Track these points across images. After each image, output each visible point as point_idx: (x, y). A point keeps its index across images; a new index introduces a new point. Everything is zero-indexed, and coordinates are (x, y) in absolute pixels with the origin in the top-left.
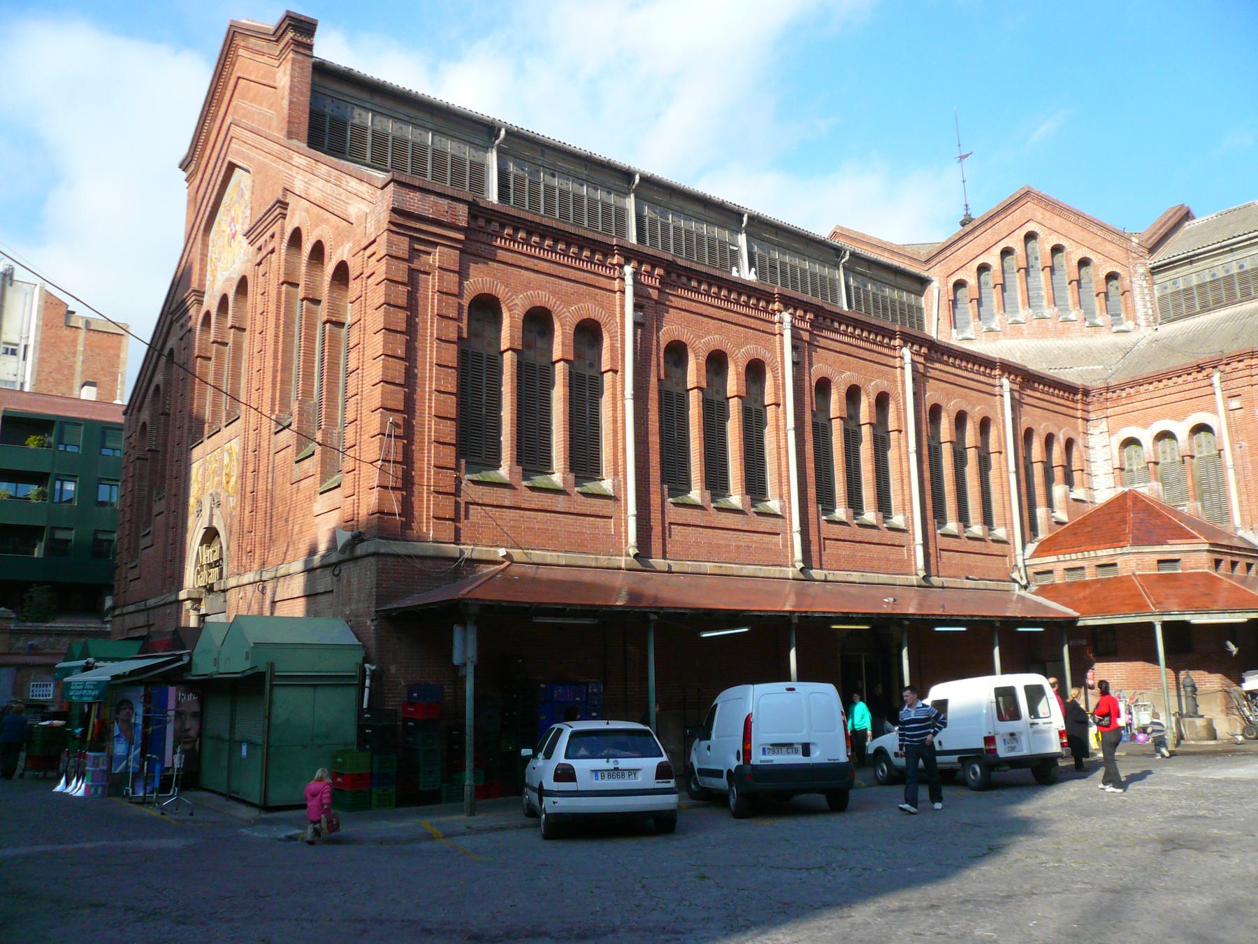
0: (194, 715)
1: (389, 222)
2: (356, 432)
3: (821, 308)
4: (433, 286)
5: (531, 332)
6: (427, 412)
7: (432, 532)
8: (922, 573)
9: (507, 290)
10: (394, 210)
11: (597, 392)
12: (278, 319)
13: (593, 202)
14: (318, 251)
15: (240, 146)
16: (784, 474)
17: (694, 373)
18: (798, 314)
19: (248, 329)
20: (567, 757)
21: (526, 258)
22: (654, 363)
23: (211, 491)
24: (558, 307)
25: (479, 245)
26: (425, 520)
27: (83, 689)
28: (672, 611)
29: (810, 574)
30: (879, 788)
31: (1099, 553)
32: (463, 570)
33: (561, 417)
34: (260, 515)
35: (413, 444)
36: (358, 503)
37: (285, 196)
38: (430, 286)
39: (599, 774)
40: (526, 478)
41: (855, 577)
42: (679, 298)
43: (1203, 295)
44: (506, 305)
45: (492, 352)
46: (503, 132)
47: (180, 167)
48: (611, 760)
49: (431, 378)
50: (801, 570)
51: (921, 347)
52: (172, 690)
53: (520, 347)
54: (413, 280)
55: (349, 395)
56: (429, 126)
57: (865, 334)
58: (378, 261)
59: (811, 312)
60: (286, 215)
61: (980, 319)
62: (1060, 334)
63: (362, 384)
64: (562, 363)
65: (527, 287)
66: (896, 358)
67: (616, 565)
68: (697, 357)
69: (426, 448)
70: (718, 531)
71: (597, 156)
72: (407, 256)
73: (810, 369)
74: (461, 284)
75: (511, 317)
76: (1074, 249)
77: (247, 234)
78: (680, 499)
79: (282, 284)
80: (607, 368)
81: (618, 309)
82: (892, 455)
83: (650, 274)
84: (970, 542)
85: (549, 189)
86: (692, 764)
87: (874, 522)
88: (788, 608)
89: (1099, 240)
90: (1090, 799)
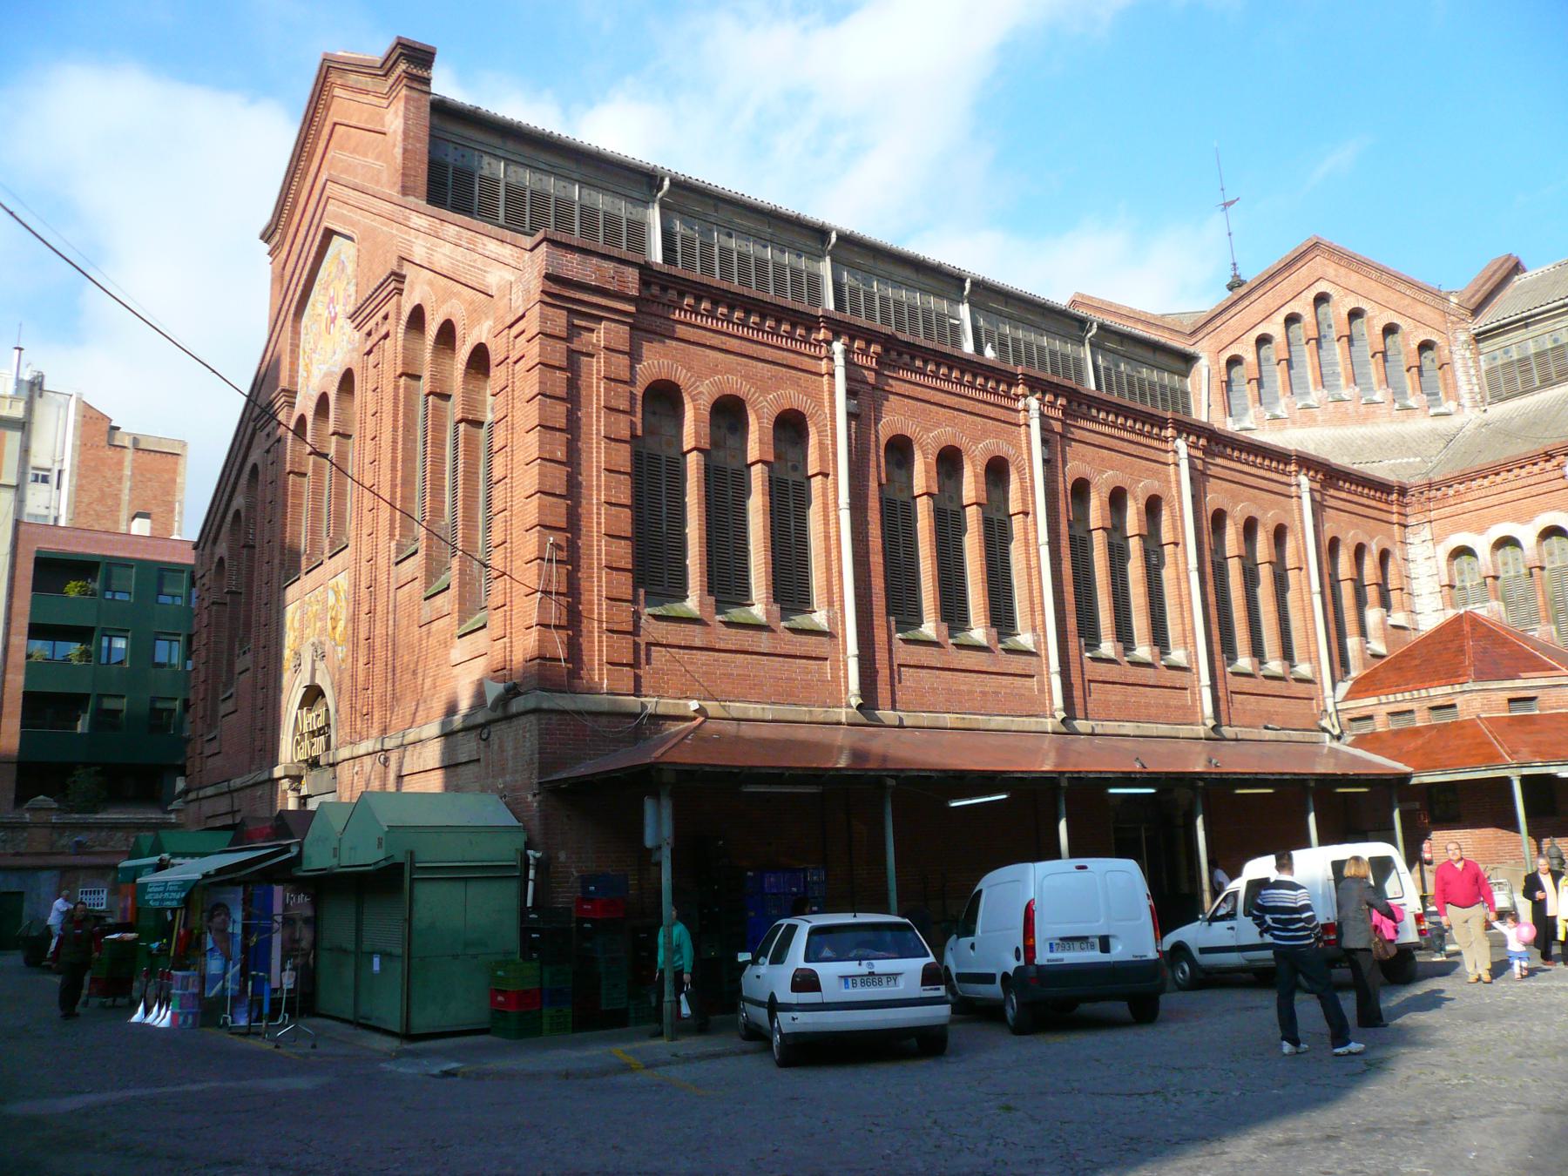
0: (307, 921)
1: (542, 291)
2: (506, 558)
3: (1075, 391)
4: (599, 372)
6: (595, 529)
7: (605, 681)
8: (1211, 723)
10: (548, 277)
11: (803, 501)
12: (395, 420)
13: (779, 267)
14: (447, 333)
16: (1037, 600)
17: (922, 475)
18: (1047, 399)
19: (356, 436)
20: (807, 959)
21: (711, 334)
22: (873, 464)
23: (312, 640)
25: (653, 318)
26: (596, 667)
27: (164, 892)
29: (1074, 726)
30: (1181, 994)
31: (1433, 692)
32: (646, 729)
33: (761, 533)
34: (379, 667)
35: (579, 571)
36: (511, 647)
38: (595, 370)
39: (850, 980)
40: (719, 611)
41: (1129, 728)
42: (902, 381)
44: (689, 394)
45: (673, 453)
46: (667, 183)
47: (262, 238)
48: (864, 963)
49: (599, 486)
50: (1063, 721)
51: (1198, 437)
52: (278, 890)
53: (708, 447)
54: (573, 363)
55: (495, 510)
56: (575, 176)
57: (1130, 423)
58: (528, 341)
59: (1063, 396)
60: (403, 290)
61: (1324, 387)
62: (1363, 419)
63: (512, 496)
64: (759, 466)
66: (1167, 452)
67: (834, 718)
69: (595, 575)
71: (783, 210)
72: (564, 335)
73: (1064, 467)
74: (632, 368)
75: (695, 409)
77: (352, 317)
78: (910, 635)
79: (400, 376)
80: (815, 471)
81: (826, 396)
82: (1167, 574)
83: (865, 352)
85: (725, 252)
86: (947, 968)
87: (1149, 659)
88: (1046, 768)
89: (1408, 301)
90: (1467, 1000)
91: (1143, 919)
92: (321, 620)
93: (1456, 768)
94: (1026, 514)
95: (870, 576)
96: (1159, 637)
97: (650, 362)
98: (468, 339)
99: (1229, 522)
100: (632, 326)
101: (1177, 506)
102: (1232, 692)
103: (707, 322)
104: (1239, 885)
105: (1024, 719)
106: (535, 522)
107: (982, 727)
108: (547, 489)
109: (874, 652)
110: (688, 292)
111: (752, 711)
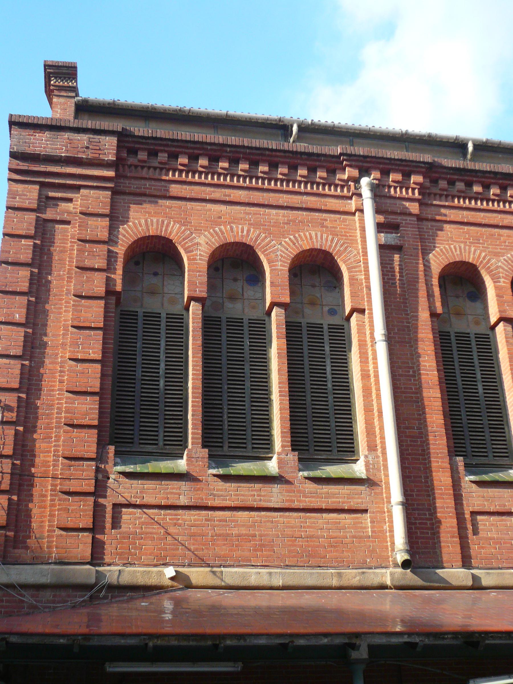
9: (183, 228)
10: (13, 155)
21: (212, 189)
24: (263, 240)
25: (143, 182)
35: (35, 432)
46: (295, 128)
53: (204, 295)
65: (217, 221)
67: (376, 581)
68: (495, 279)
81: (358, 232)
83: (403, 184)
95: (424, 413)
109: (434, 498)
110: (181, 153)
111: (253, 577)
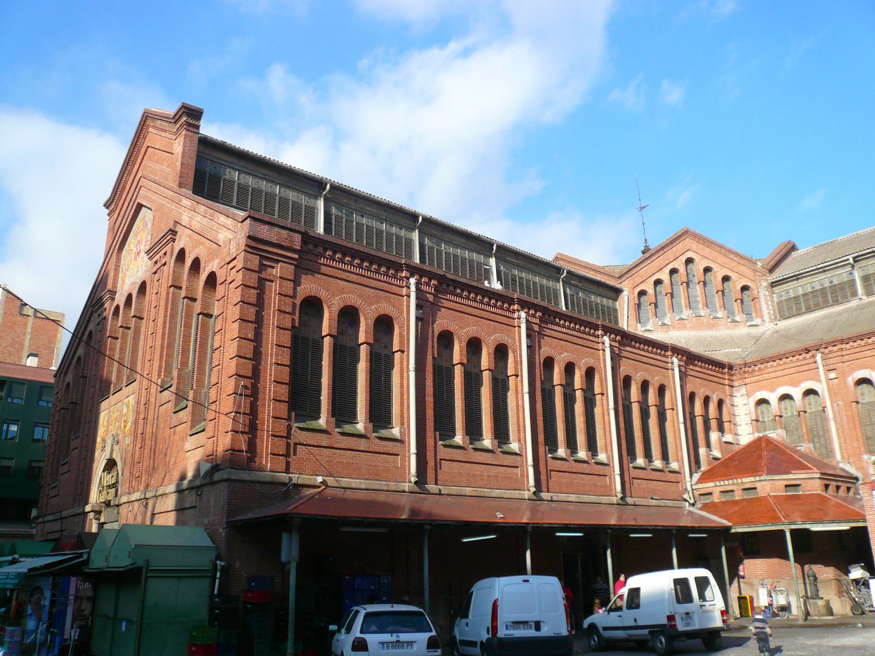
0: (89, 598)
1: (246, 245)
2: (217, 392)
3: (547, 308)
4: (275, 290)
5: (343, 323)
7: (269, 464)
8: (620, 495)
10: (249, 237)
11: (390, 365)
12: (166, 311)
13: (389, 235)
14: (196, 265)
15: (146, 192)
16: (521, 424)
17: (458, 353)
18: (530, 312)
20: (362, 632)
21: (341, 272)
22: (430, 346)
23: (113, 432)
24: (363, 306)
25: (308, 262)
27: (7, 578)
28: (440, 523)
29: (541, 496)
31: (744, 480)
32: (291, 492)
33: (364, 383)
34: (147, 451)
36: (217, 442)
37: (175, 226)
38: (273, 289)
39: (385, 645)
40: (338, 426)
41: (572, 497)
43: (806, 301)
45: (316, 337)
46: (328, 186)
47: (104, 206)
48: (394, 635)
49: (272, 354)
50: (534, 493)
52: (73, 580)
53: (336, 334)
54: (261, 286)
55: (214, 365)
56: (278, 181)
57: (577, 327)
58: (237, 272)
59: (540, 311)
60: (175, 239)
61: (657, 317)
62: (711, 327)
63: (223, 358)
64: (365, 345)
66: (598, 343)
67: (401, 489)
69: (267, 404)
70: (475, 465)
71: (393, 204)
74: (295, 289)
75: (329, 313)
76: (719, 269)
77: (147, 252)
78: (447, 442)
79: (170, 287)
80: (397, 349)
81: (405, 308)
82: (597, 411)
83: (428, 284)
84: (653, 472)
85: (359, 226)
86: (455, 636)
87: (586, 458)
88: (525, 520)
89: (735, 264)
91: (560, 612)
92: (118, 421)
93: (756, 525)
94: (517, 376)
95: (425, 409)
96: (592, 447)
97: (305, 286)
98: (206, 268)
99: (633, 383)
100: (296, 266)
101: (603, 373)
102: (633, 478)
103: (339, 265)
104: (624, 591)
105: (512, 491)
106: (234, 373)
107: (487, 495)
108: (242, 355)
110: (329, 248)
